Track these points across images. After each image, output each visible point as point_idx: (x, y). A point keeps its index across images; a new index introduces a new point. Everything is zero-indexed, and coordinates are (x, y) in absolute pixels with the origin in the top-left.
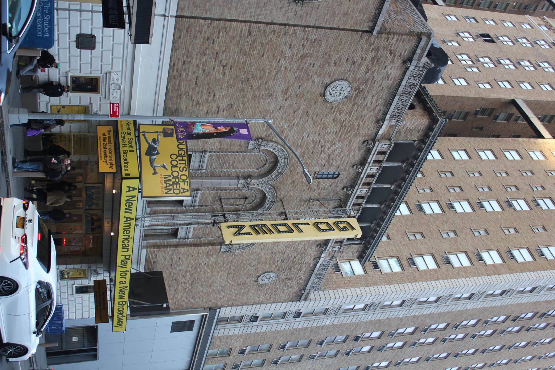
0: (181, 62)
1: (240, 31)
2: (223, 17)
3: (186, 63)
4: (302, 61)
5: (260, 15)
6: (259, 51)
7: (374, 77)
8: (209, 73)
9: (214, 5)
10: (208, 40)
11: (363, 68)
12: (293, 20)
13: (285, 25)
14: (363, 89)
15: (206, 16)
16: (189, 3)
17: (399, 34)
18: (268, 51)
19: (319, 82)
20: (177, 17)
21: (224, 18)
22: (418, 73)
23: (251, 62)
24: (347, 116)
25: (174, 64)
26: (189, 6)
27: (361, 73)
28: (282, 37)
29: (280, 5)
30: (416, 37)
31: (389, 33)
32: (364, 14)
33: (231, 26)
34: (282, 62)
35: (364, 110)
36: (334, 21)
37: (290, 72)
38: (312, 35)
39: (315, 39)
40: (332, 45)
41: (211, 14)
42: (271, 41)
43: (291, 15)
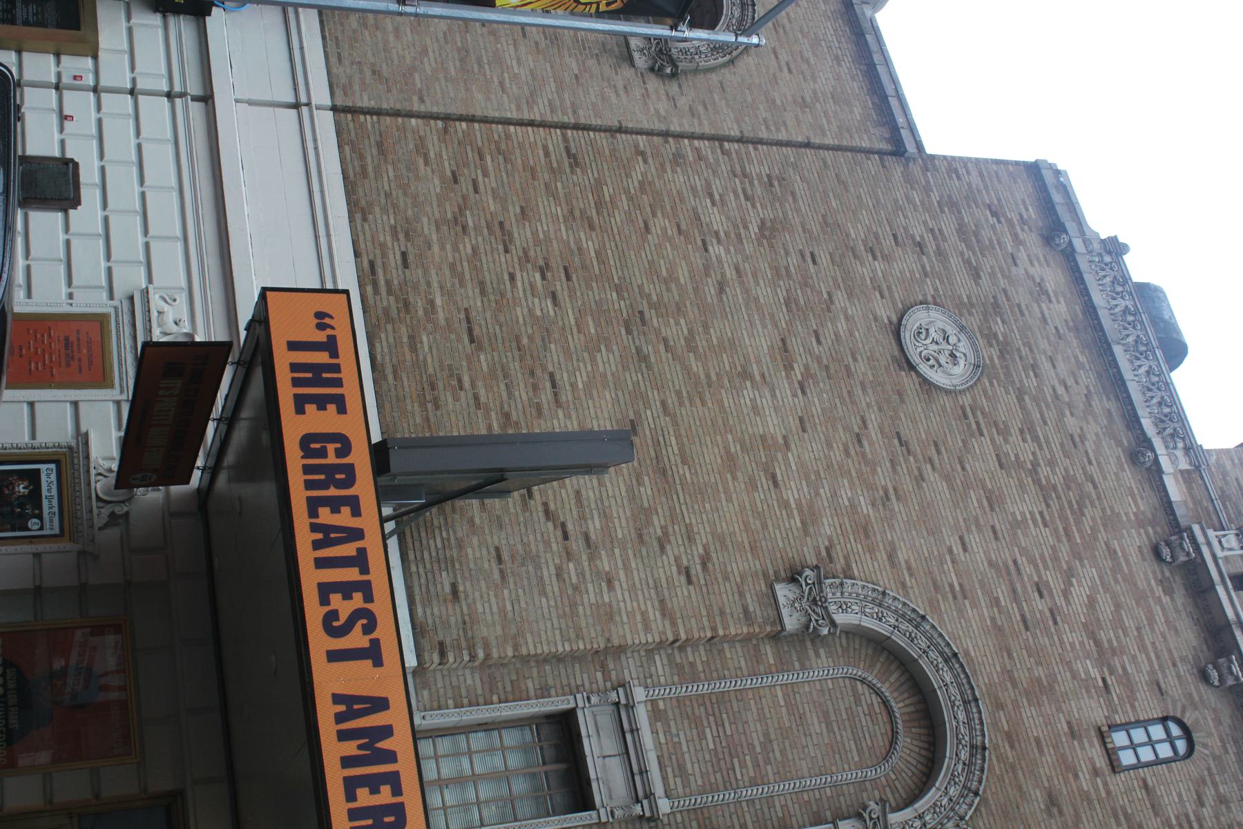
0: (394, 259)
1: (541, 152)
3: (411, 258)
4: (771, 246)
7: (1005, 290)
8: (502, 295)
9: (437, 79)
12: (675, 120)
14: (1005, 337)
15: (423, 109)
16: (361, 71)
20: (334, 108)
21: (479, 113)
24: (1030, 446)
25: (372, 265)
26: (363, 81)
29: (620, 84)
34: (715, 249)
35: (1063, 415)
36: (785, 124)
39: (769, 176)
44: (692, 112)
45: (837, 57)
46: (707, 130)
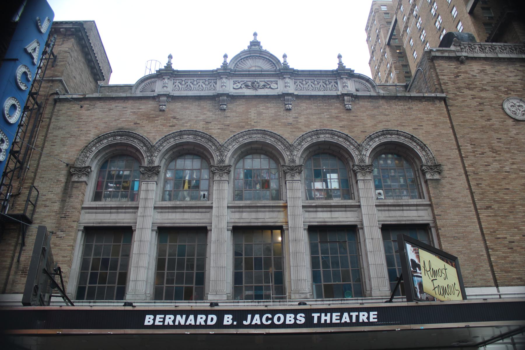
1: (490, 218)
2: (481, 238)
5: (465, 202)
6: (504, 194)
9: (471, 249)
10: (512, 248)
11: (483, 94)
13: (467, 176)
14: (505, 88)
15: (486, 255)
16: (477, 275)
17: (437, 76)
18: (501, 186)
19: (514, 128)
22: (467, 48)
23: (520, 199)
26: (480, 275)
27: (490, 95)
28: (481, 175)
29: (448, 186)
30: (434, 61)
31: (440, 84)
32: (429, 110)
33: (487, 228)
34: (507, 169)
36: (447, 134)
37: (515, 159)
38: (468, 149)
39: (471, 145)
40: (471, 128)
41: (482, 251)
42: (489, 185)
43: (455, 174)
44: (454, 163)
45: (409, 108)
46: (459, 160)
